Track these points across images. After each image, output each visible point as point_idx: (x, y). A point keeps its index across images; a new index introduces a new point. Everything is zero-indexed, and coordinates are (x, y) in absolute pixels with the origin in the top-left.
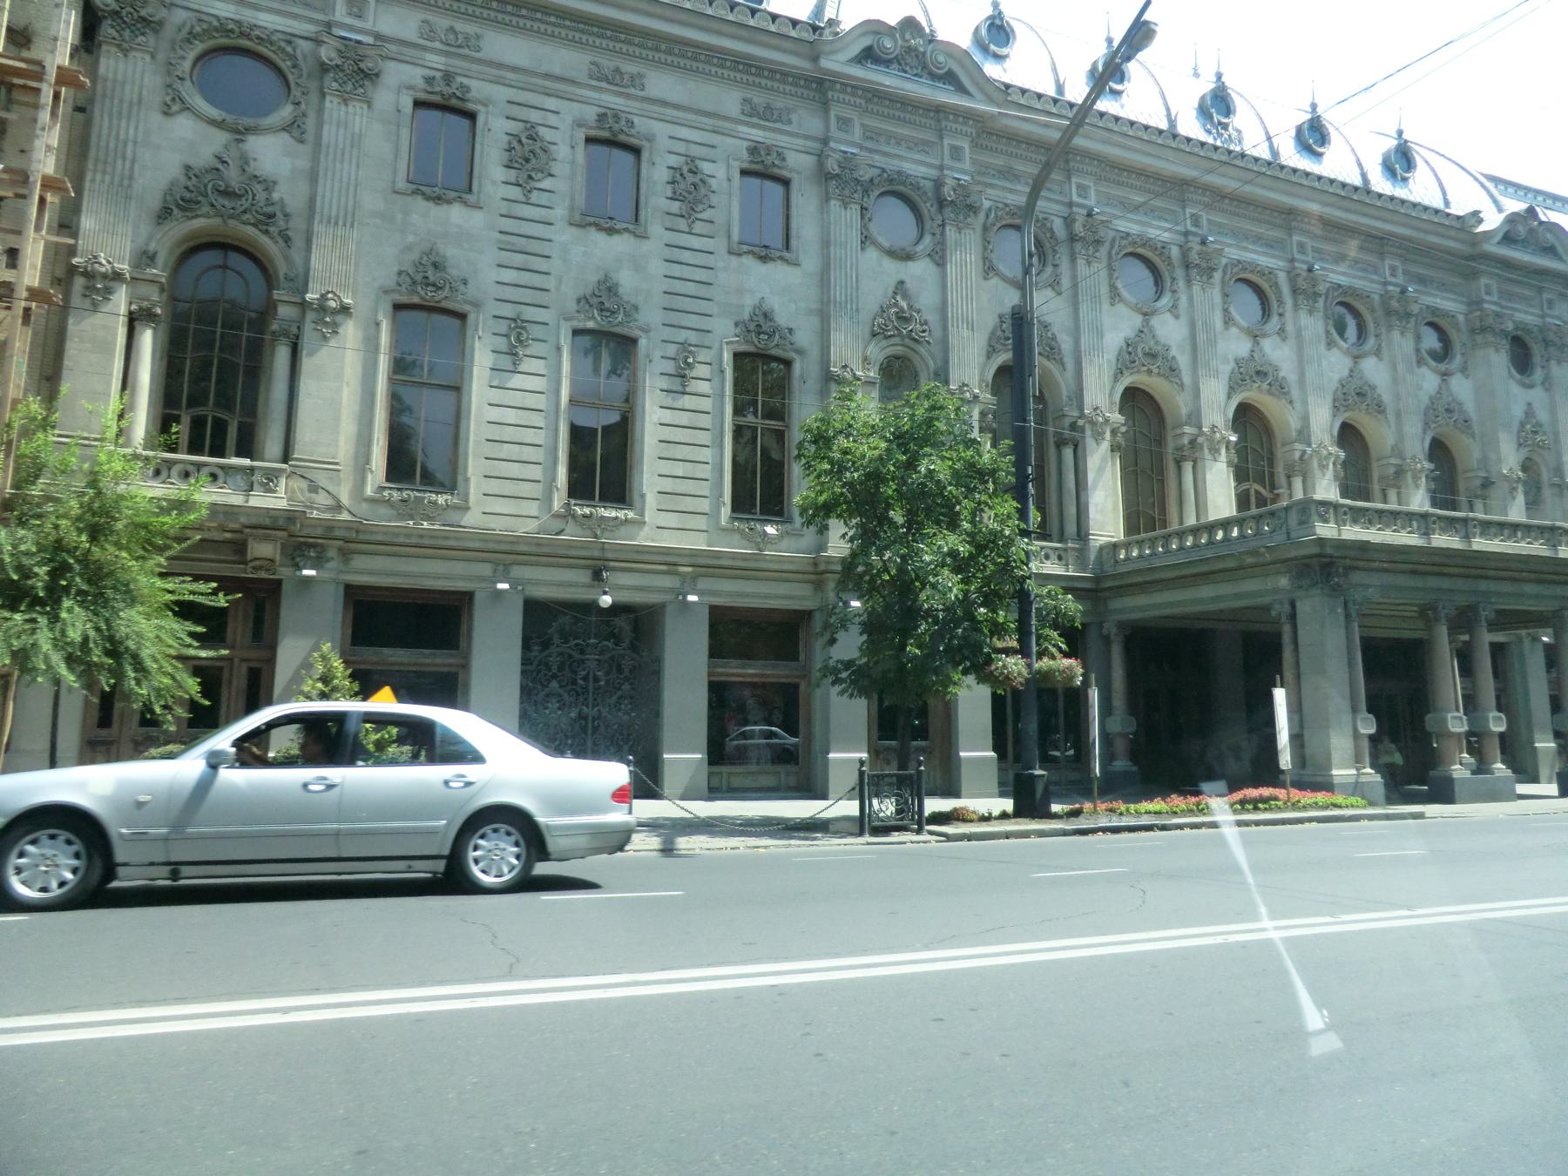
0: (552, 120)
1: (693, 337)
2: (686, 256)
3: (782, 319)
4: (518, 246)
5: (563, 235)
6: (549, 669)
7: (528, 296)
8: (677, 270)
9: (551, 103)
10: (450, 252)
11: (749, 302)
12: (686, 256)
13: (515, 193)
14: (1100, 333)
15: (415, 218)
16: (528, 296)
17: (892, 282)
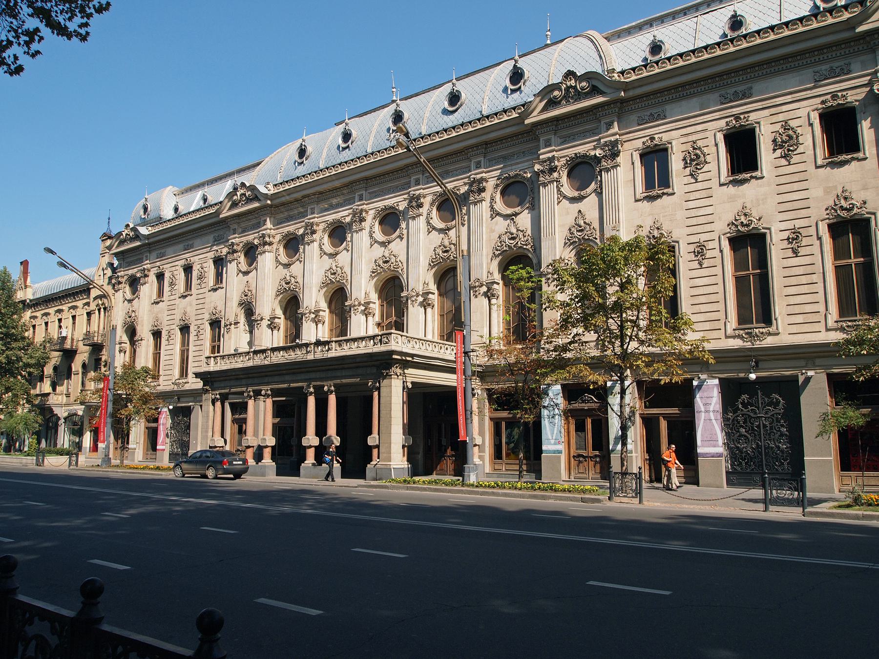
6: (739, 423)
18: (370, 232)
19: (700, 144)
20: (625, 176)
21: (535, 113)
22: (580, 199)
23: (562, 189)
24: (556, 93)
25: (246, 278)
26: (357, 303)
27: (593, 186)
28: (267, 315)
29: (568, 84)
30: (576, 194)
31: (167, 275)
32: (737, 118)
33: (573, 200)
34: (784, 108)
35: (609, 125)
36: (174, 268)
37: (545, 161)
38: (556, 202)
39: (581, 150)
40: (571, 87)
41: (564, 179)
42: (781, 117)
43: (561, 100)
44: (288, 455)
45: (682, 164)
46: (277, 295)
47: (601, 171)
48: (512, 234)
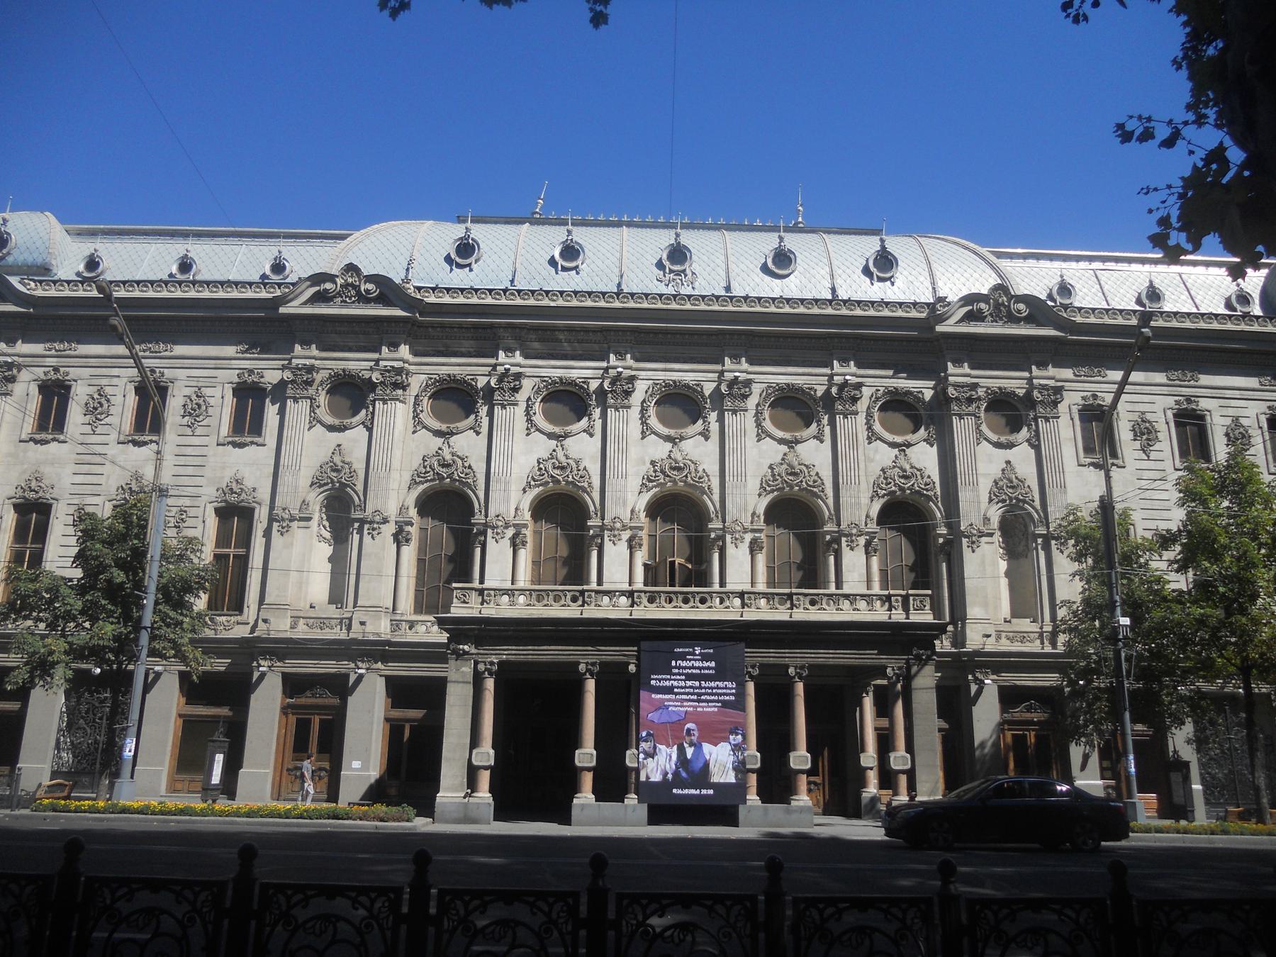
0: (115, 381)
1: (187, 502)
2: (189, 451)
3: (248, 483)
4: (90, 459)
5: (113, 450)
7: (88, 489)
8: (182, 460)
9: (115, 372)
10: (46, 470)
11: (227, 476)
12: (189, 451)
13: (88, 429)
14: (510, 456)
15: (30, 454)
16: (88, 489)
17: (333, 446)
18: (756, 415)
19: (1149, 416)
20: (1065, 431)
21: (952, 321)
22: (1010, 446)
23: (317, 411)
24: (328, 286)
25: (335, 437)
26: (618, 525)
27: (1024, 432)
28: (392, 510)
29: (350, 280)
30: (337, 422)
31: (80, 393)
32: (1189, 399)
33: (331, 428)
34: (1233, 403)
35: (394, 346)
36: (104, 382)
37: (389, 371)
38: (307, 426)
39: (352, 366)
40: (352, 285)
41: (322, 399)
42: (1231, 412)
43: (335, 297)
44: (776, 785)
45: (1131, 435)
46: (414, 483)
47: (374, 401)
48: (792, 467)
